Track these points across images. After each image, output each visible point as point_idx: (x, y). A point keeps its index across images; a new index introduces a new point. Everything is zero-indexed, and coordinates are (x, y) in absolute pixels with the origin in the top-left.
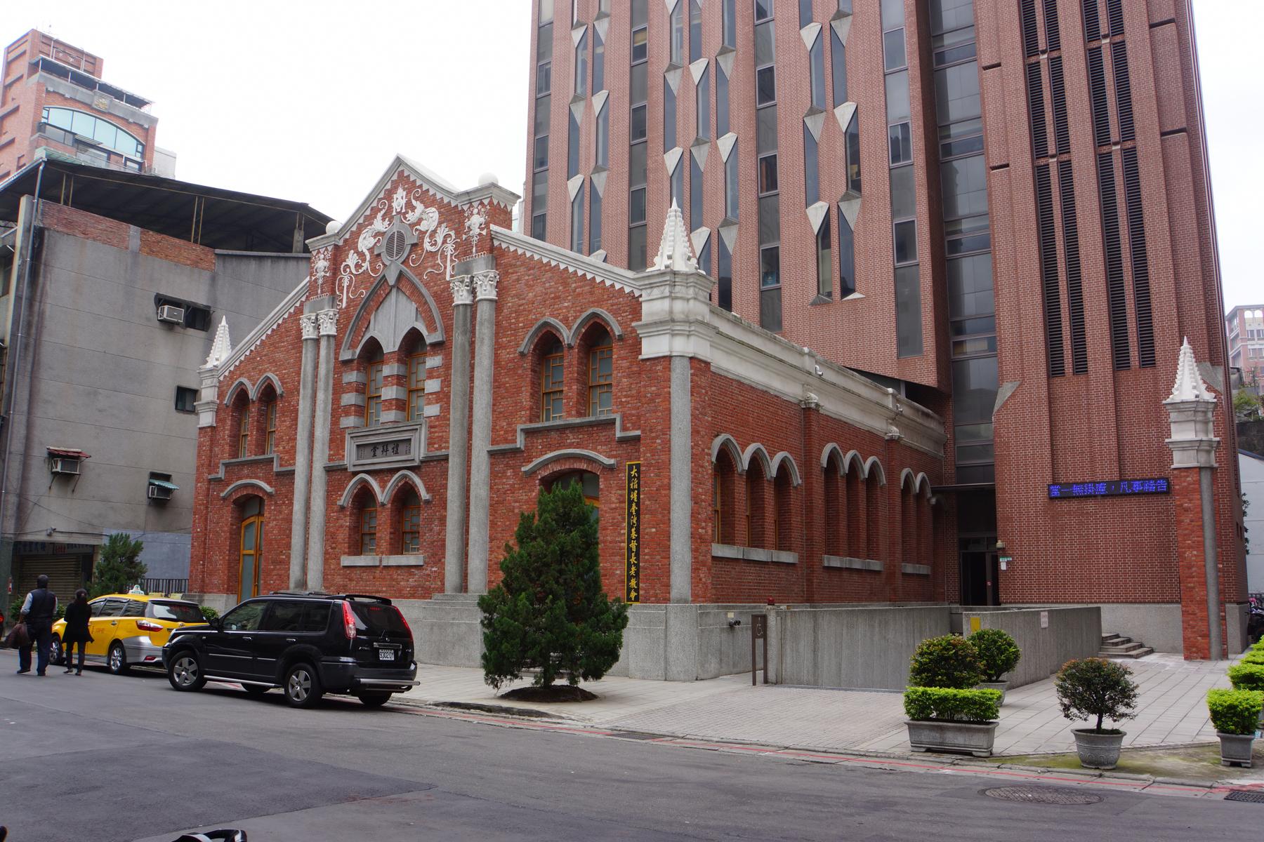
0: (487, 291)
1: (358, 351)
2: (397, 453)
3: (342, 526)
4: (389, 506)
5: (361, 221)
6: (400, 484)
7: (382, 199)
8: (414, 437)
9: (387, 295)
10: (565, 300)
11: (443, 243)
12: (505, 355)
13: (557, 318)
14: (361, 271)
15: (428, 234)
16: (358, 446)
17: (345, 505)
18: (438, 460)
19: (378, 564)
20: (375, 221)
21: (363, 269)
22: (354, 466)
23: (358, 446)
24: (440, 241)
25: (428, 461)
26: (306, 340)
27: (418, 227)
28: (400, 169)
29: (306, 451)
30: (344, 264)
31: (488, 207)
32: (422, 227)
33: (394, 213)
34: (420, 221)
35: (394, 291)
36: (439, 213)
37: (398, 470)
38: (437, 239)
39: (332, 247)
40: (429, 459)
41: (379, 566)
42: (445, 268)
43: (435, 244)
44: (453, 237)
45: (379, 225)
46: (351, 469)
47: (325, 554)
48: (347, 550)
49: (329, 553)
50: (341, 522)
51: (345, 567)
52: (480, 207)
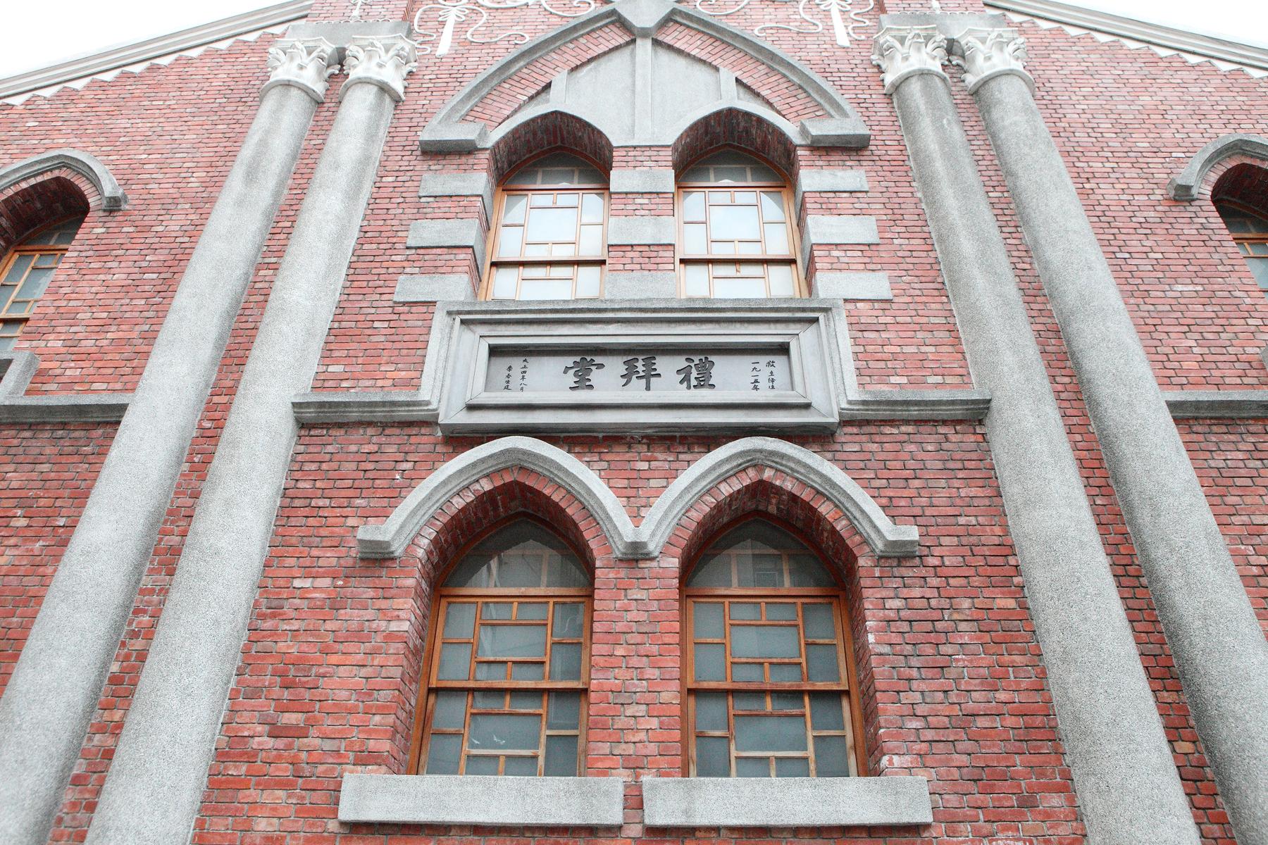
2: (704, 382)
3: (359, 635)
4: (673, 563)
6: (726, 490)
8: (804, 342)
9: (611, 50)
12: (1107, 192)
16: (495, 351)
17: (398, 549)
18: (918, 422)
19: (613, 814)
22: (471, 408)
23: (495, 351)
25: (868, 422)
26: (287, 85)
29: (206, 352)
35: (644, 46)
40: (884, 413)
41: (612, 830)
46: (453, 415)
47: (221, 755)
48: (385, 746)
49: (250, 757)
50: (353, 617)
51: (357, 828)
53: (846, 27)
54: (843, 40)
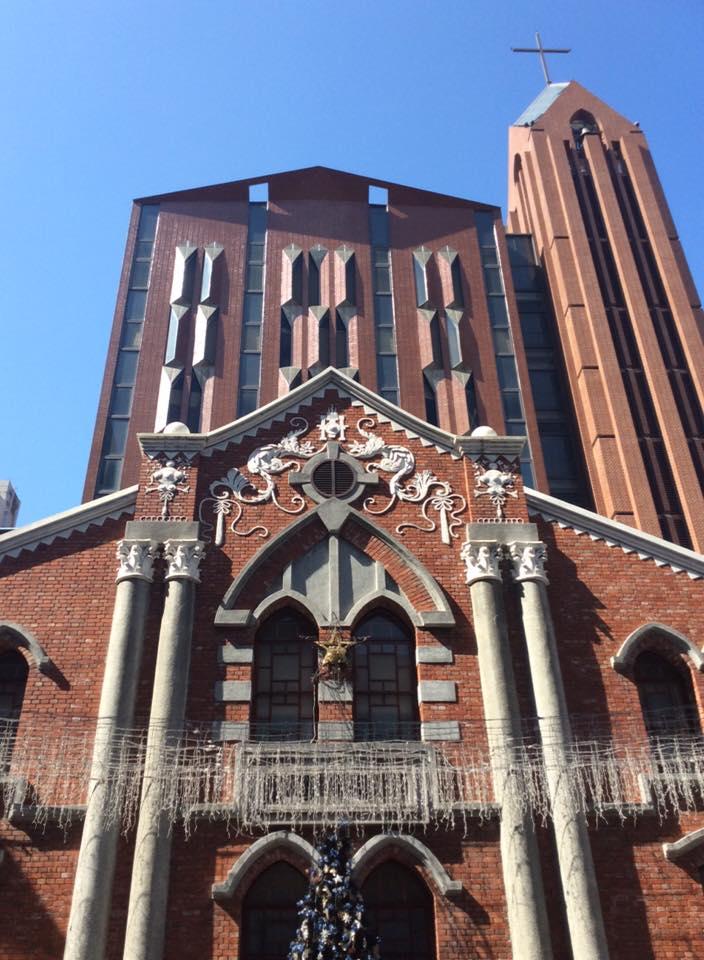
0: (527, 568)
1: (257, 614)
5: (253, 433)
7: (295, 415)
10: (675, 604)
11: (429, 494)
13: (669, 623)
14: (254, 499)
15: (396, 477)
20: (285, 440)
21: (260, 498)
24: (422, 491)
27: (375, 464)
28: (331, 387)
30: (216, 483)
31: (515, 465)
32: (384, 464)
33: (323, 437)
34: (377, 456)
36: (415, 455)
37: (372, 830)
38: (418, 487)
39: (195, 454)
42: (438, 527)
43: (413, 491)
44: (448, 489)
45: (289, 444)
52: (500, 463)
53: (449, 525)
54: (446, 539)
